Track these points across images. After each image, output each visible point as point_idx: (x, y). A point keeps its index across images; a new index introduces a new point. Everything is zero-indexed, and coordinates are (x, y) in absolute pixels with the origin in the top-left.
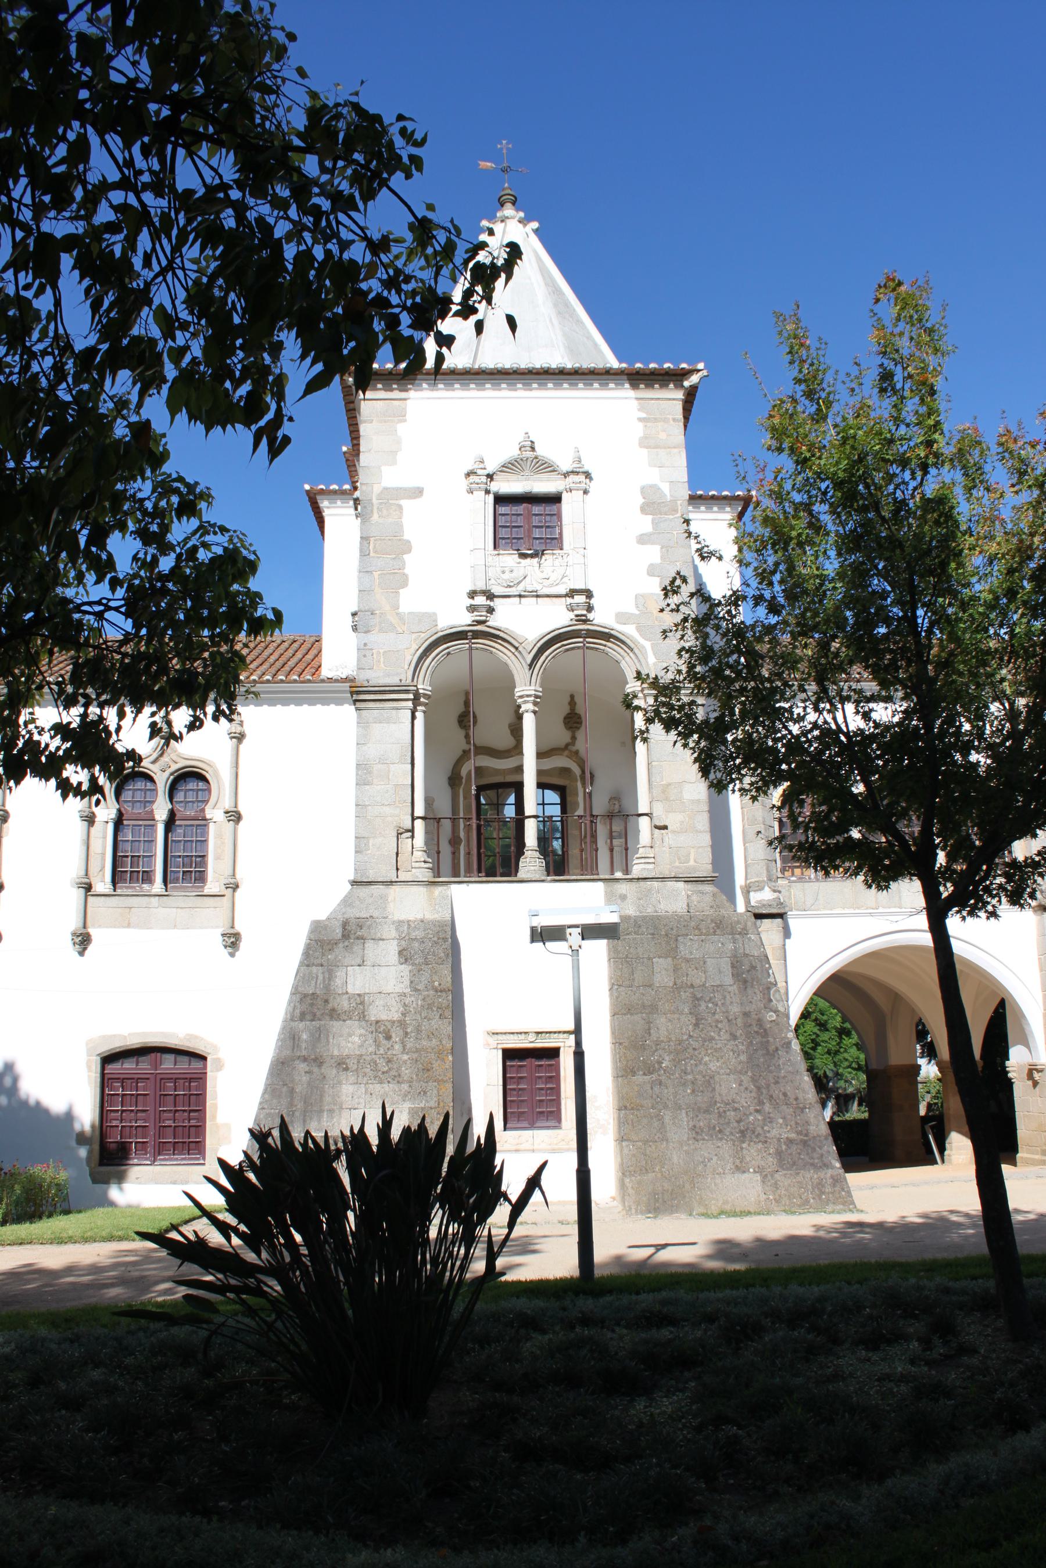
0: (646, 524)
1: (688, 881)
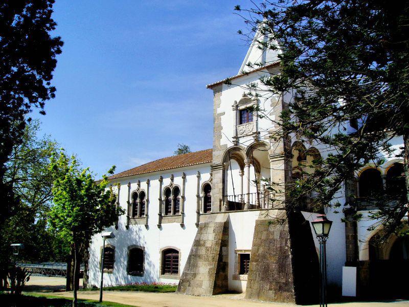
1: (279, 209)
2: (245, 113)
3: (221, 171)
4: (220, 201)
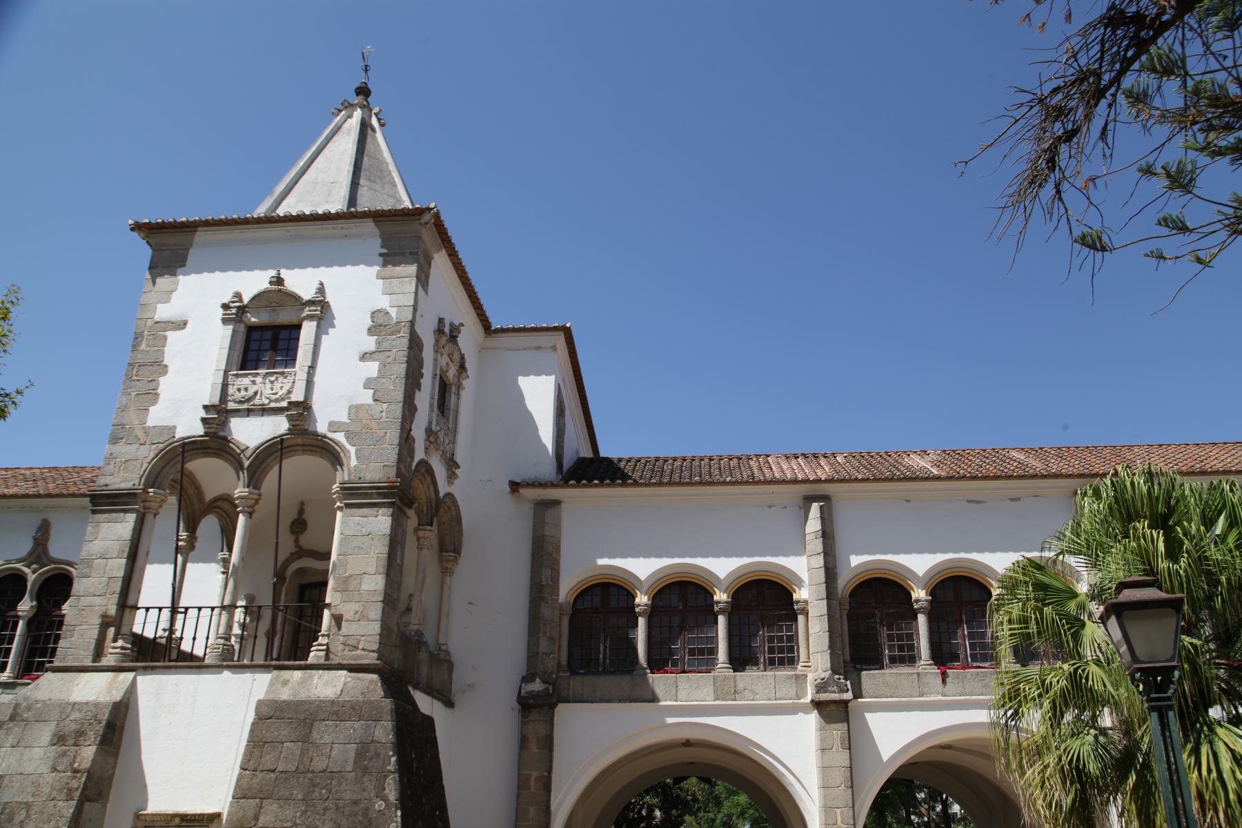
0: (370, 343)
2: (266, 338)
3: (131, 518)
4: (104, 626)
